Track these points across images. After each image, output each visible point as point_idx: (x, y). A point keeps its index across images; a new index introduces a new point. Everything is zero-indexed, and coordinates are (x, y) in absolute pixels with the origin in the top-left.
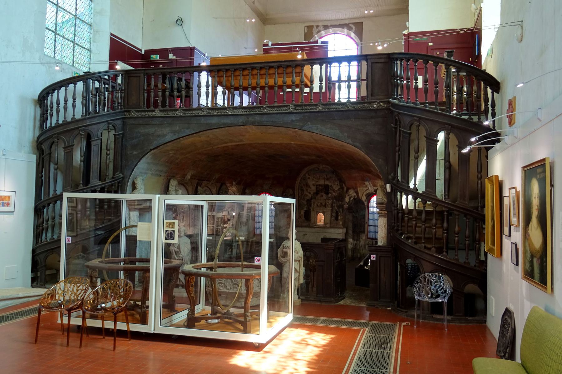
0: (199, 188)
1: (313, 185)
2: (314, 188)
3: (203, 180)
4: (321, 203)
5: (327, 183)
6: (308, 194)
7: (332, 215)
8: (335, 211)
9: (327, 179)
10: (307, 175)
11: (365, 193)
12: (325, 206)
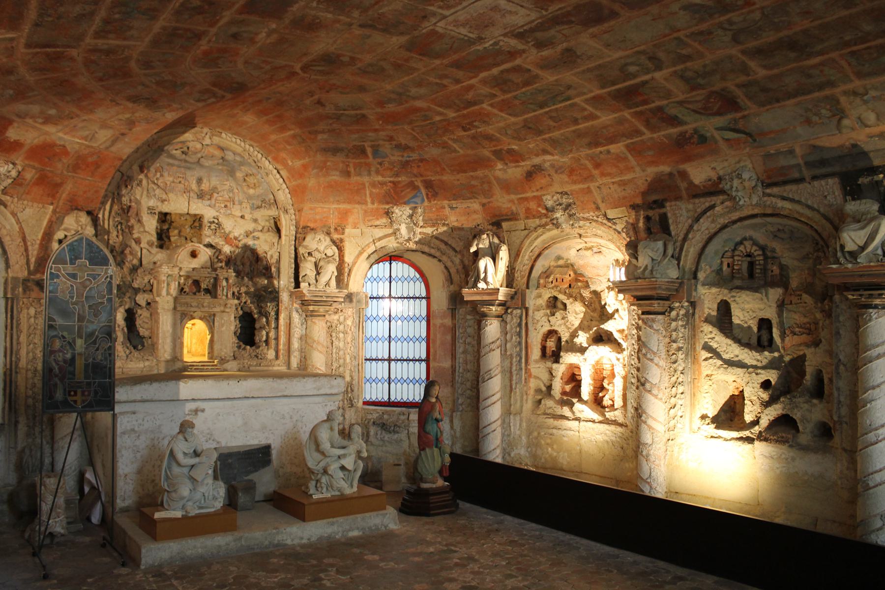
4: (196, 283)
5: (198, 208)
9: (201, 196)
11: (372, 249)
12: (212, 291)
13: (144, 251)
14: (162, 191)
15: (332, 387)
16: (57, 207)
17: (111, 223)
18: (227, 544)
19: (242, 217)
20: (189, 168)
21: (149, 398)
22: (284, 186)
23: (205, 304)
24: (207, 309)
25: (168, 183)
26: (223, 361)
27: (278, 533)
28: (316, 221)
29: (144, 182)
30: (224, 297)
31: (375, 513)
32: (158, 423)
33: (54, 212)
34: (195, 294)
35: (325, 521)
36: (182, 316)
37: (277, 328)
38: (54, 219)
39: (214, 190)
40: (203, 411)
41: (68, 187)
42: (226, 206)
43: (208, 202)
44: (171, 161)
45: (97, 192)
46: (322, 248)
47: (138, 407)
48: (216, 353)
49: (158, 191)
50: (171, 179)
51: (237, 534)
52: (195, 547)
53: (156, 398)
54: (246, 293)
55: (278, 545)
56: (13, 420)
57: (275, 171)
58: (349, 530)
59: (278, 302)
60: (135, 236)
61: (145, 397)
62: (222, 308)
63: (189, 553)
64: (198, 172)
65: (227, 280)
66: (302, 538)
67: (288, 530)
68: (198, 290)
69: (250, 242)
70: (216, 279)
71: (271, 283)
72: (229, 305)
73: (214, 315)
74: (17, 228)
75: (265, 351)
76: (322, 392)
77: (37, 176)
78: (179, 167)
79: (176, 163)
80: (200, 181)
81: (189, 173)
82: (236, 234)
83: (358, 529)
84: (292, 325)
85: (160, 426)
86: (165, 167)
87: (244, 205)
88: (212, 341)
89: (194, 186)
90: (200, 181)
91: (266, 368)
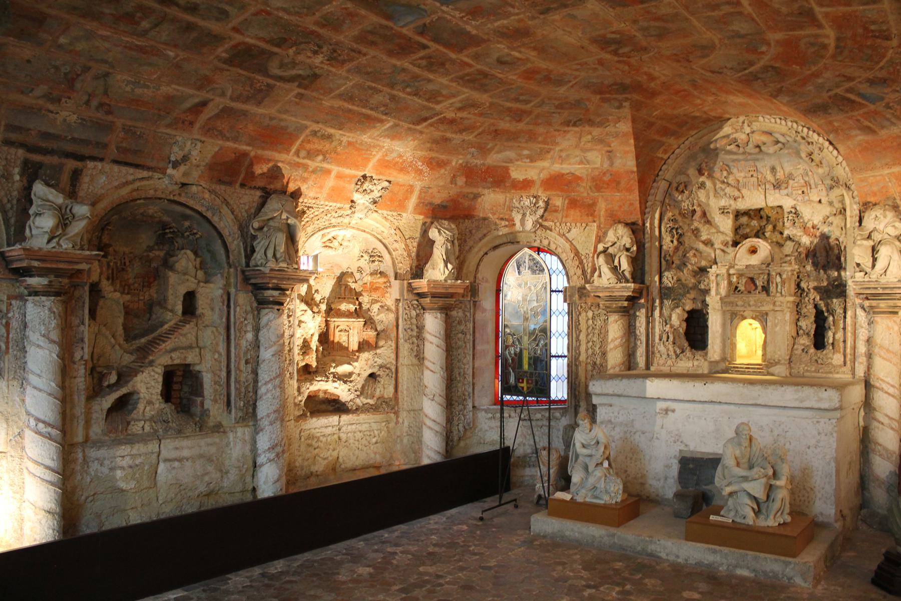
0: (39, 188)
1: (723, 211)
2: (726, 224)
3: (82, 158)
4: (752, 280)
5: (775, 199)
6: (701, 247)
7: (798, 328)
8: (810, 310)
9: (777, 186)
10: (692, 172)
13: (718, 252)
14: (732, 189)
15: (820, 400)
16: (600, 224)
17: (663, 229)
18: (600, 537)
19: (820, 201)
20: (758, 160)
21: (619, 393)
22: (840, 159)
23: (752, 303)
24: (753, 308)
25: (741, 179)
26: (777, 363)
27: (651, 542)
28: (875, 194)
29: (709, 184)
30: (778, 295)
31: (773, 557)
32: (632, 417)
33: (599, 227)
34: (750, 292)
35: (706, 546)
36: (733, 317)
37: (844, 329)
38: (601, 234)
39: (790, 176)
40: (673, 411)
41: (602, 207)
42: (803, 192)
43: (785, 192)
44: (735, 157)
45: (631, 204)
46: (881, 227)
47: (614, 400)
48: (768, 356)
49: (728, 190)
50: (742, 174)
51: (613, 530)
52: (572, 530)
53: (625, 393)
54: (815, 288)
55: (651, 555)
56: (573, 403)
57: (827, 143)
58: (736, 566)
59: (845, 296)
60: (704, 238)
61: (616, 392)
62: (771, 307)
63: (567, 533)
64: (769, 162)
65: (780, 275)
66: (678, 557)
67: (662, 542)
68: (753, 287)
69: (826, 229)
70: (769, 274)
71: (839, 275)
72: (777, 304)
73: (767, 314)
74: (568, 245)
75: (831, 355)
76: (807, 404)
77: (567, 202)
78: (746, 160)
79: (741, 157)
80: (773, 170)
81: (759, 165)
82: (816, 222)
83: (748, 568)
84: (857, 326)
85: (633, 421)
86: (731, 164)
87: (820, 187)
88: (765, 342)
89: (769, 177)
90: (773, 170)
91: (824, 375)
